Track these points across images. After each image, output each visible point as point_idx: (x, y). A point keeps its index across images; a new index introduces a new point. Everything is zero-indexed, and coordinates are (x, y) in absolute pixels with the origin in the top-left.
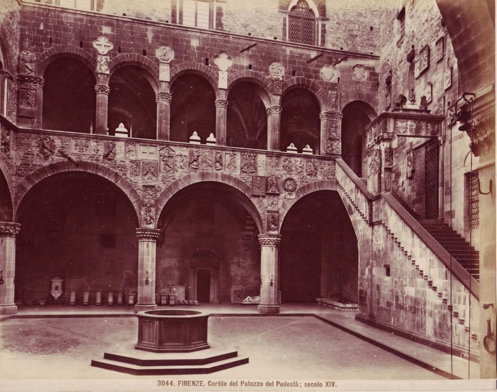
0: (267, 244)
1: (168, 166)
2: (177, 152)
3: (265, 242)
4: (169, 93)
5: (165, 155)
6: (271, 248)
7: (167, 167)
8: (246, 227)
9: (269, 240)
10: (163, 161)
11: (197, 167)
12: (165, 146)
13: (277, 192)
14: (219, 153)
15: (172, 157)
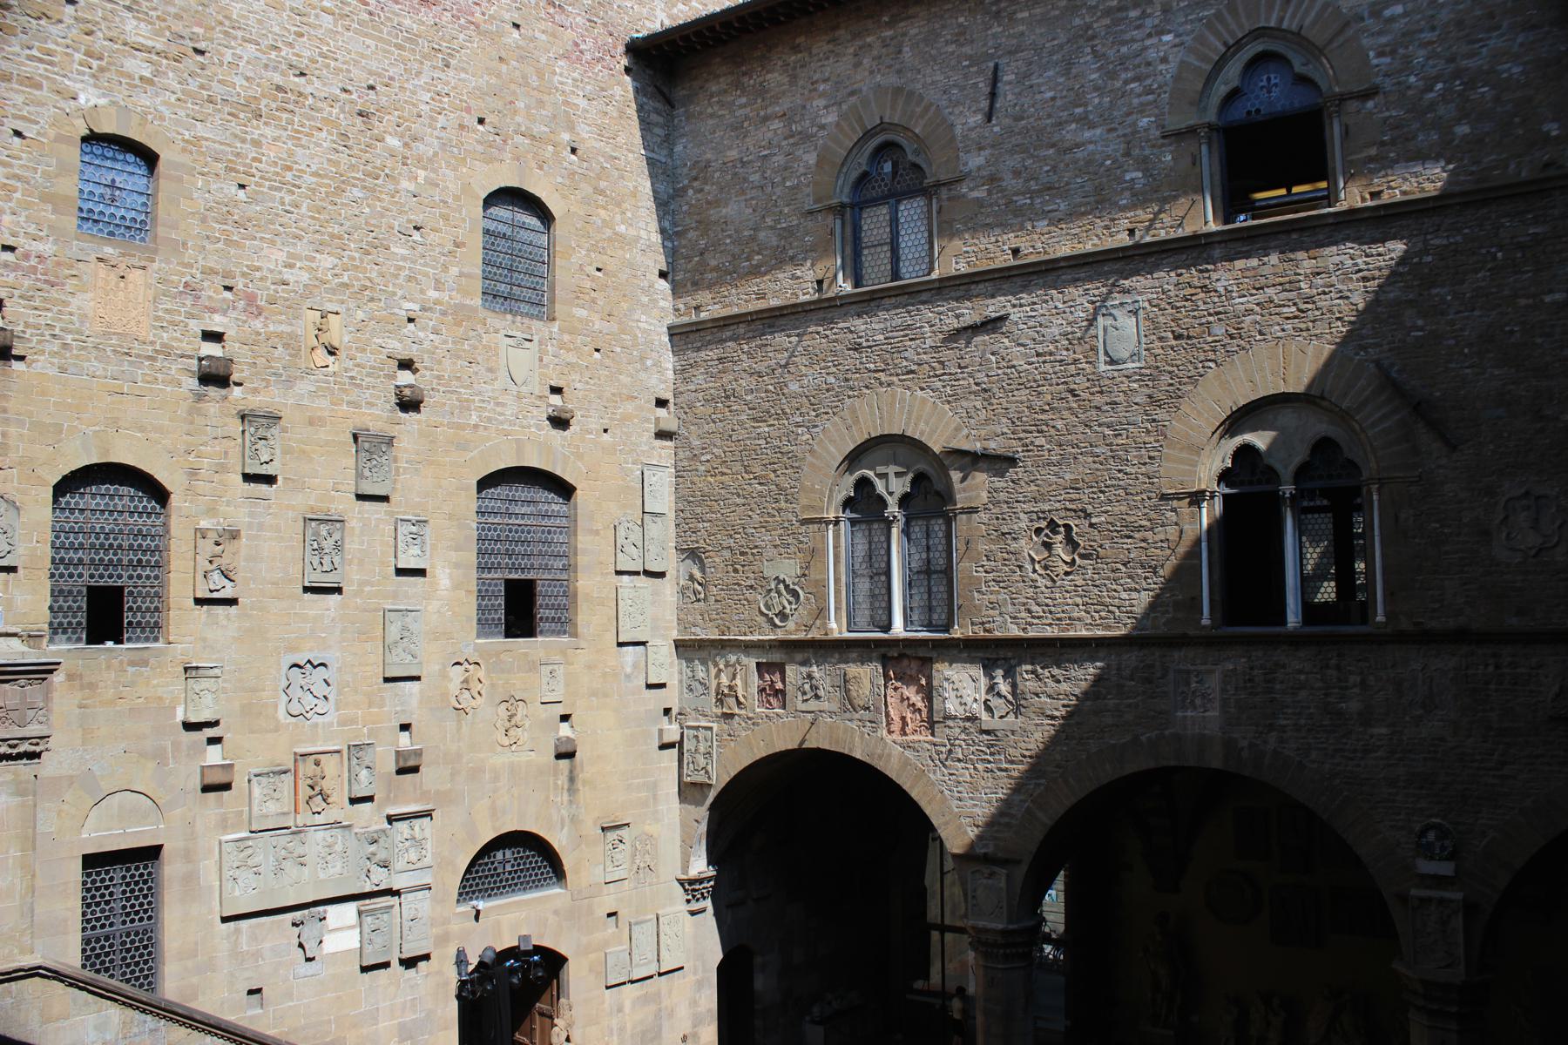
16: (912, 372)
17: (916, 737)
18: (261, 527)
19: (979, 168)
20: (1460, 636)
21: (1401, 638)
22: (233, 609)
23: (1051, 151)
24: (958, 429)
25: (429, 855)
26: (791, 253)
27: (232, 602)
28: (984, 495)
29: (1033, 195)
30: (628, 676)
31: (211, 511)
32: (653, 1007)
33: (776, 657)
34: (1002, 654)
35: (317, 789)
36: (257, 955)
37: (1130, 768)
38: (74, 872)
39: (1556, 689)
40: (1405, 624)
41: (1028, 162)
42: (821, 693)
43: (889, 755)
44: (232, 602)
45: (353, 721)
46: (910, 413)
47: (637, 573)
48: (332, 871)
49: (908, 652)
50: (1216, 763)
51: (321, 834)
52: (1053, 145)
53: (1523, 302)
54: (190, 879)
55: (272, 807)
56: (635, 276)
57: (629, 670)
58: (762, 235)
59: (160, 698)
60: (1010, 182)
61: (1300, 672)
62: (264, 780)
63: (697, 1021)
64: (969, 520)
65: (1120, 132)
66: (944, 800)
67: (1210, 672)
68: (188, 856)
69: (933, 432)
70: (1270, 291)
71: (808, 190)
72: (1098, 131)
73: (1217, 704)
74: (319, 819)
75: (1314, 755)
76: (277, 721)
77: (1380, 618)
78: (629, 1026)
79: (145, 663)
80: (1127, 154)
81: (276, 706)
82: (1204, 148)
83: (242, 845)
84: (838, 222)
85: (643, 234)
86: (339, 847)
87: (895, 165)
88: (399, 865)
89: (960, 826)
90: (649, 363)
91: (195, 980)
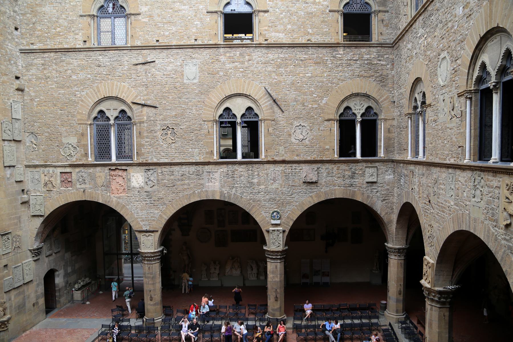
16: (120, 76)
17: (121, 195)
19: (146, 12)
20: (284, 162)
21: (268, 162)
23: (171, 10)
24: (136, 96)
26: (73, 29)
28: (145, 118)
29: (164, 23)
30: (8, 179)
32: (22, 296)
33: (68, 170)
34: (151, 167)
37: (192, 201)
39: (305, 175)
40: (269, 159)
41: (163, 13)
42: (86, 181)
43: (112, 201)
46: (119, 91)
47: (11, 140)
49: (119, 167)
50: (218, 198)
52: (172, 9)
53: (301, 75)
56: (5, 27)
57: (8, 176)
58: (61, 21)
60: (156, 18)
61: (242, 172)
63: (38, 298)
64: (140, 126)
65: (194, 9)
66: (132, 214)
67: (217, 172)
69: (127, 97)
70: (236, 64)
71: (81, 8)
72: (187, 7)
73: (218, 181)
75: (245, 194)
77: (263, 157)
78: (13, 305)
80: (195, 16)
82: (219, 18)
84: (92, 21)
85: (8, 11)
87: (114, 5)
89: (138, 222)
90: (12, 62)
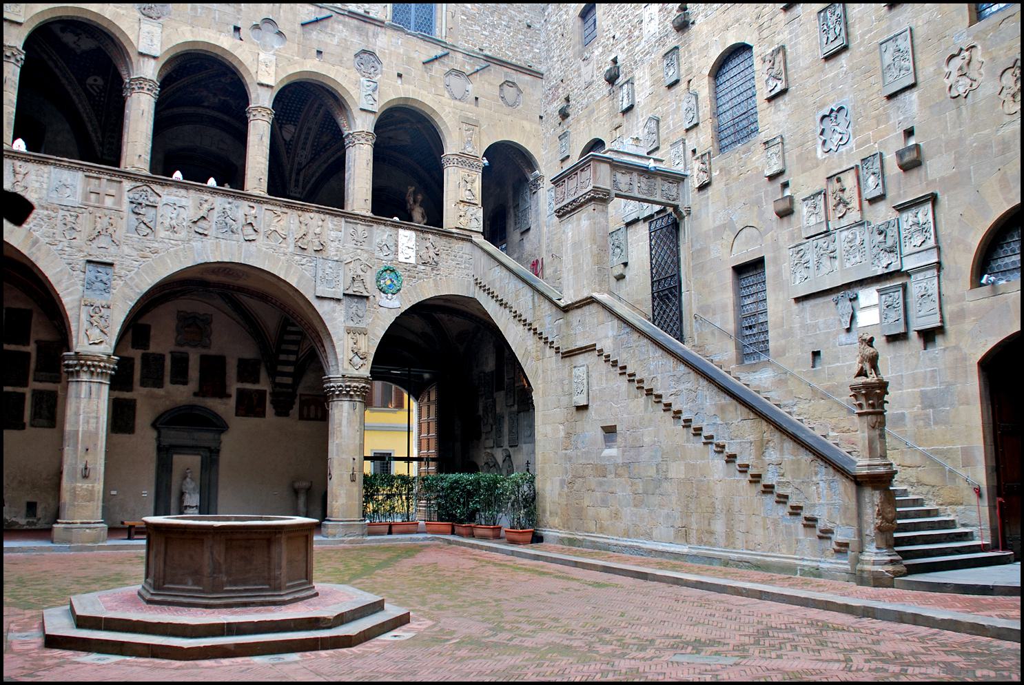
0: (345, 395)
1: (145, 224)
2: (165, 199)
3: (340, 391)
4: (155, 80)
5: (140, 201)
6: (352, 403)
7: (142, 224)
8: (280, 368)
9: (349, 386)
10: (134, 212)
11: (206, 233)
12: (139, 184)
13: (365, 294)
14: (253, 207)
15: (156, 207)
18: (797, 36)
22: (787, 98)
25: (933, 237)
27: (784, 92)
31: (771, 44)
35: (838, 199)
36: (815, 326)
38: (729, 274)
44: (784, 92)
45: (867, 141)
48: (853, 260)
51: (845, 233)
54: (778, 274)
55: (813, 220)
59: (757, 168)
62: (810, 202)
68: (775, 260)
74: (844, 222)
76: (816, 158)
79: (749, 150)
81: (816, 150)
83: (797, 249)
86: (858, 241)
88: (906, 251)
91: (783, 342)
